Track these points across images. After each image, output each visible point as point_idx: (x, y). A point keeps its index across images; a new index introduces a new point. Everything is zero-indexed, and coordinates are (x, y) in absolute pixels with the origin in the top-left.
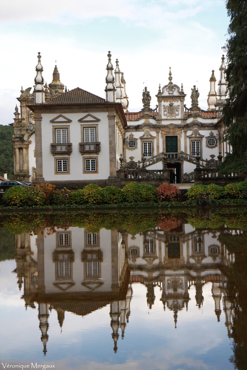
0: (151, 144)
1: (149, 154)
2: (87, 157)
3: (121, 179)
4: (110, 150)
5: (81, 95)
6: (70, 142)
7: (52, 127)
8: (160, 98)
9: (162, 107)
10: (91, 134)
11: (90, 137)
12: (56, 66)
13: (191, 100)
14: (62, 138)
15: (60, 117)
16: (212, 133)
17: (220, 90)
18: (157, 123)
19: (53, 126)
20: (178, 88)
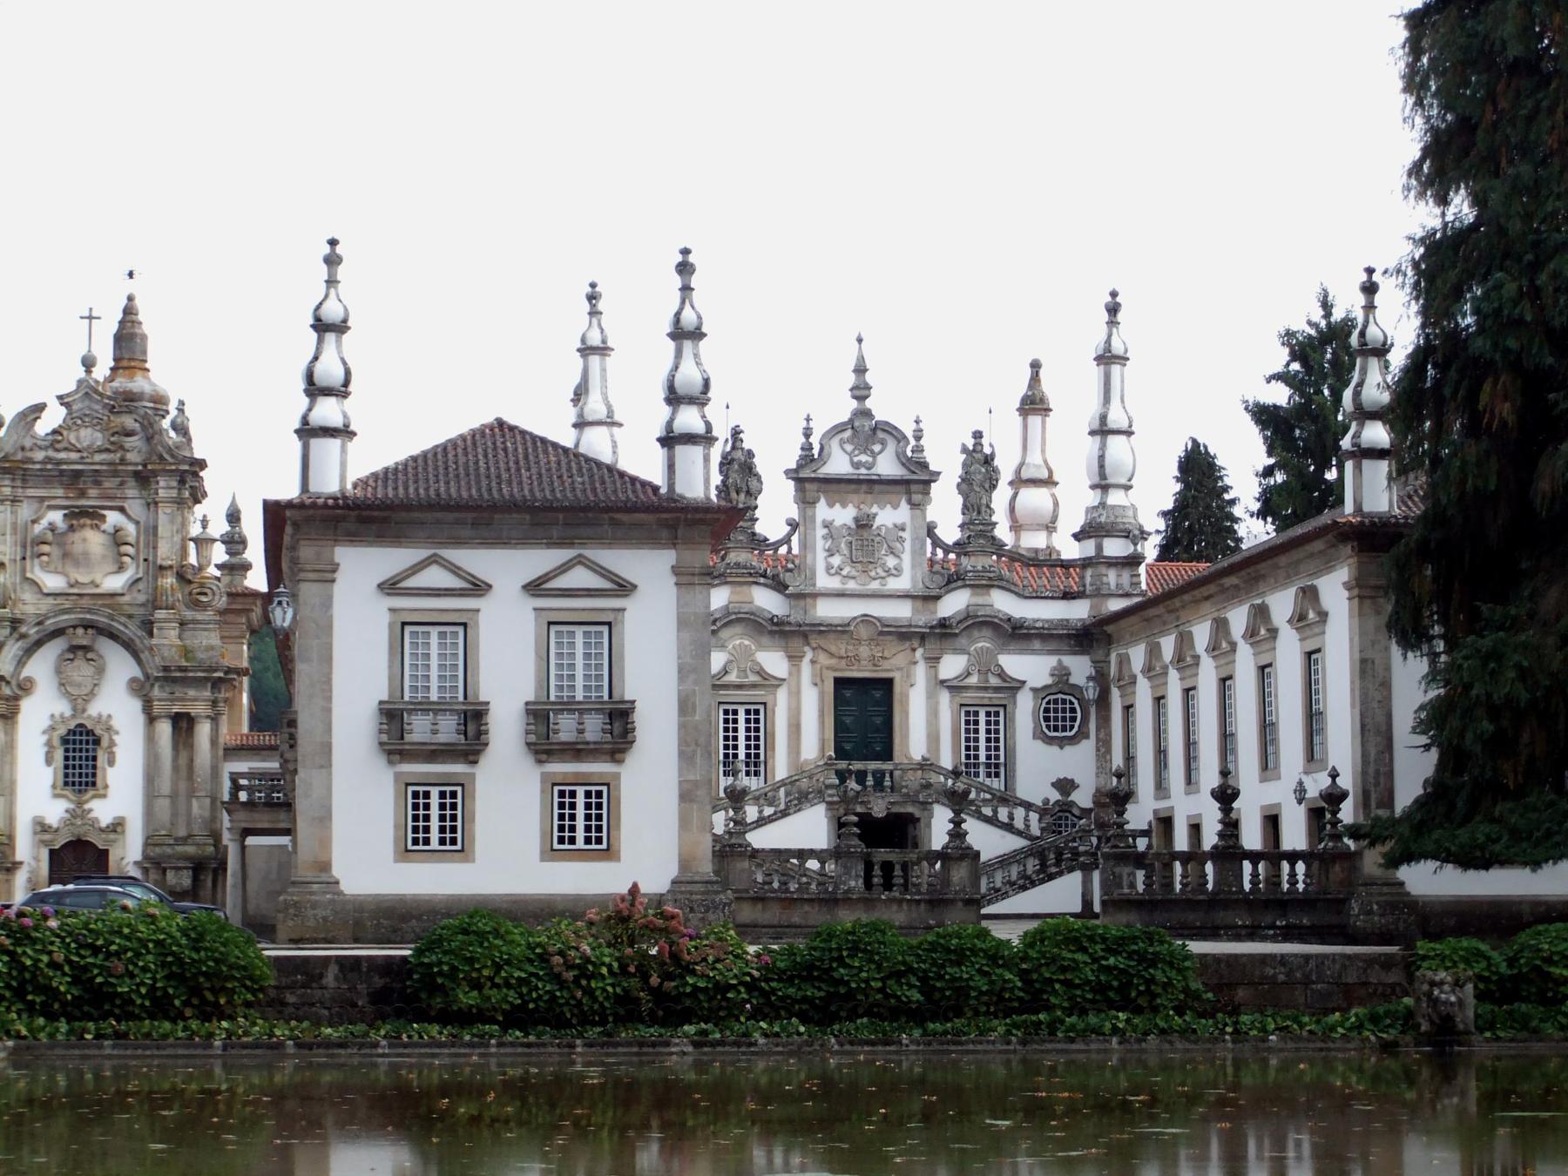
0: (762, 717)
1: (747, 765)
2: (565, 774)
3: (735, 891)
4: (683, 742)
5: (526, 457)
6: (477, 696)
7: (385, 618)
8: (808, 486)
9: (821, 532)
10: (587, 656)
11: (579, 673)
12: (130, 298)
13: (960, 500)
14: (434, 673)
15: (429, 565)
16: (1065, 668)
17: (1102, 458)
19: (392, 610)
20: (900, 437)
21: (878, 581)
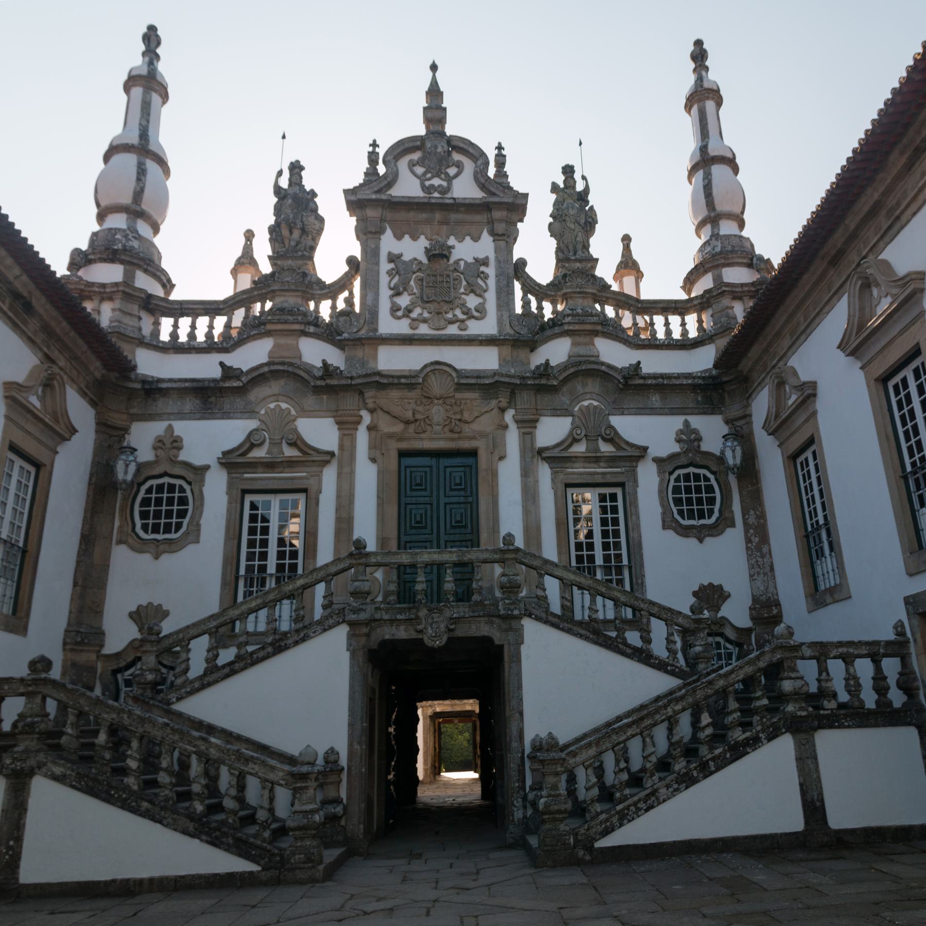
16: (695, 432)
18: (347, 359)
21: (458, 323)
